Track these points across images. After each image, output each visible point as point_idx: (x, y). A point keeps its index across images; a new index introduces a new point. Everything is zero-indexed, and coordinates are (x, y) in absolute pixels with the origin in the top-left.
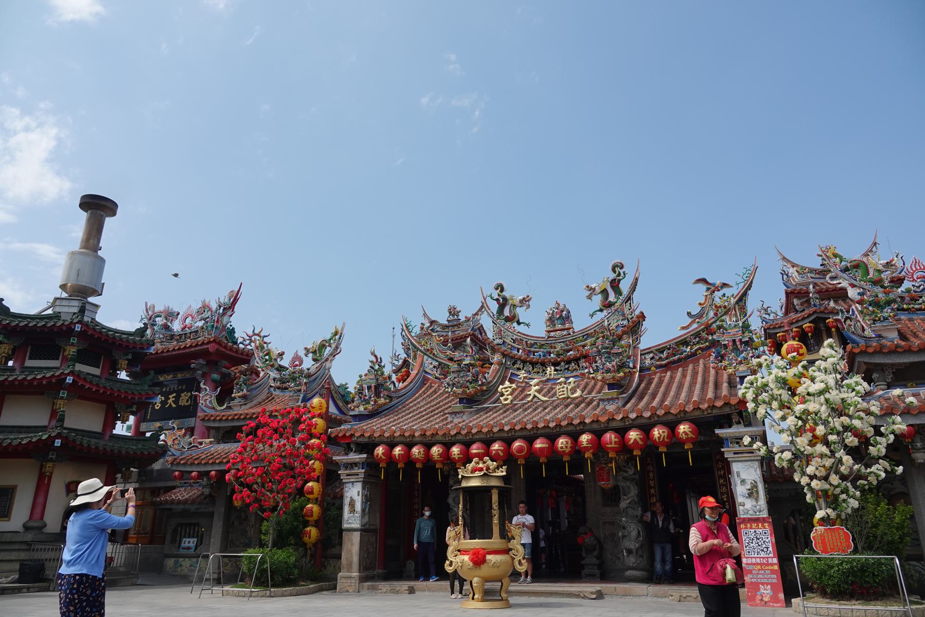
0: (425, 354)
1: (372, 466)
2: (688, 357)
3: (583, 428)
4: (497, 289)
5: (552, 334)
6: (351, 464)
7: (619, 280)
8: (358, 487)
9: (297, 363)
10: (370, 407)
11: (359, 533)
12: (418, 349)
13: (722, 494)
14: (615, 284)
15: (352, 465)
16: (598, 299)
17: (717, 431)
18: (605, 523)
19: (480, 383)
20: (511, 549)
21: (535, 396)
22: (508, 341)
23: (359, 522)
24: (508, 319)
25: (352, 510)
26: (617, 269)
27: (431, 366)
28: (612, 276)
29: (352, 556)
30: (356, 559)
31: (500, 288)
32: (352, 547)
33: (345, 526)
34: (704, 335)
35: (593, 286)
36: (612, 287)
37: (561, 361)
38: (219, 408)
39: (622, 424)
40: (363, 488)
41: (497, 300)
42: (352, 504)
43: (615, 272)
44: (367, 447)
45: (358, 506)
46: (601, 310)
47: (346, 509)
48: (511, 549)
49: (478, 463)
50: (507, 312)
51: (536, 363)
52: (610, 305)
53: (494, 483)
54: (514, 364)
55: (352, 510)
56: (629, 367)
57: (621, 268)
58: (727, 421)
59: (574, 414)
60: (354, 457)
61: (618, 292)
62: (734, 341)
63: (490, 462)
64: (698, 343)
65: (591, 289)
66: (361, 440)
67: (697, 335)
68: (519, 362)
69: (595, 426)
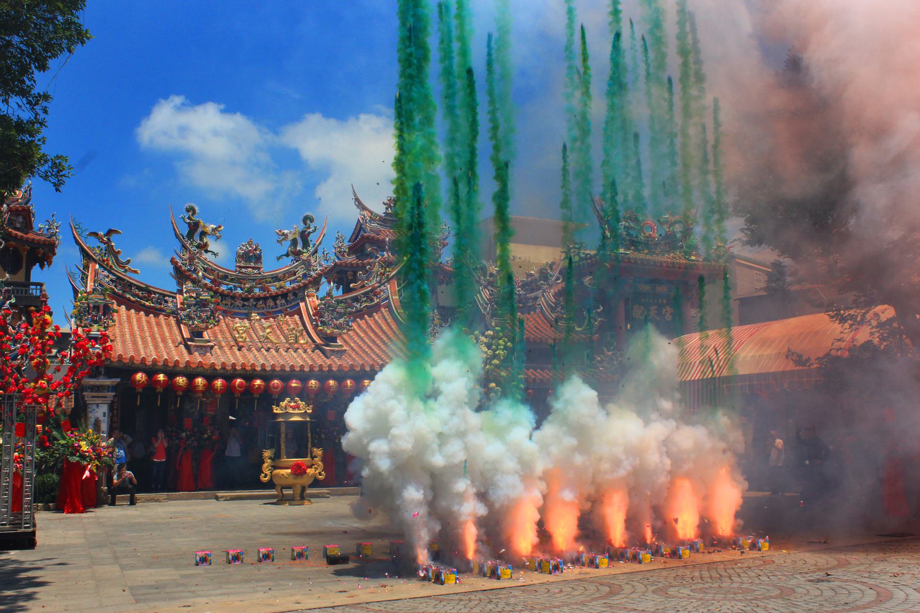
3: (330, 374)
4: (188, 211)
7: (310, 233)
8: (104, 408)
14: (304, 236)
15: (98, 388)
16: (286, 246)
26: (308, 222)
28: (302, 226)
31: (191, 210)
35: (286, 231)
41: (189, 224)
43: (305, 223)
46: (287, 255)
50: (196, 237)
51: (227, 296)
52: (297, 254)
61: (306, 244)
65: (283, 234)
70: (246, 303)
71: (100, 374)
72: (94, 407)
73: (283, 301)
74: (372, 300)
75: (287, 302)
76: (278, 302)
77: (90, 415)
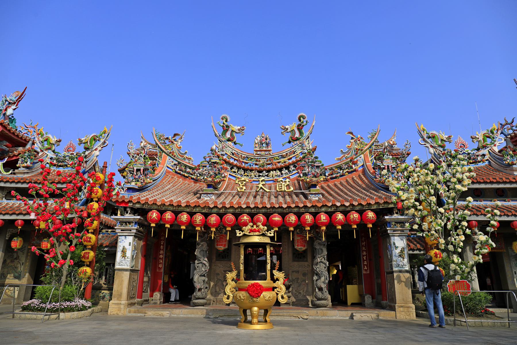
0: (168, 155)
1: (143, 225)
2: (341, 176)
5: (259, 153)
6: (126, 223)
7: (303, 126)
8: (130, 239)
9: (72, 149)
10: (139, 184)
11: (128, 273)
12: (163, 151)
13: (364, 256)
17: (386, 217)
18: (293, 272)
19: (223, 175)
20: (276, 288)
21: (261, 188)
22: (229, 154)
23: (129, 264)
24: (229, 140)
25: (124, 255)
27: (173, 164)
29: (122, 289)
30: (125, 291)
32: (122, 283)
33: (117, 267)
34: (351, 164)
36: (298, 129)
37: (264, 170)
38: (5, 173)
39: (330, 210)
40: (134, 240)
42: (124, 251)
44: (143, 211)
45: (129, 254)
47: (119, 255)
48: (276, 288)
49: (252, 226)
53: (267, 240)
54: (231, 169)
55: (124, 255)
56: (325, 176)
57: (304, 119)
58: (390, 211)
59: (283, 202)
60: (128, 216)
62: (388, 166)
63: (261, 227)
64: (347, 168)
66: (138, 206)
67: (346, 164)
68: (235, 168)
69: (313, 210)
70: (260, 174)
71: (127, 213)
72: (123, 238)
73: (287, 171)
74: (352, 167)
75: (290, 171)
76: (283, 172)
77: (119, 244)
